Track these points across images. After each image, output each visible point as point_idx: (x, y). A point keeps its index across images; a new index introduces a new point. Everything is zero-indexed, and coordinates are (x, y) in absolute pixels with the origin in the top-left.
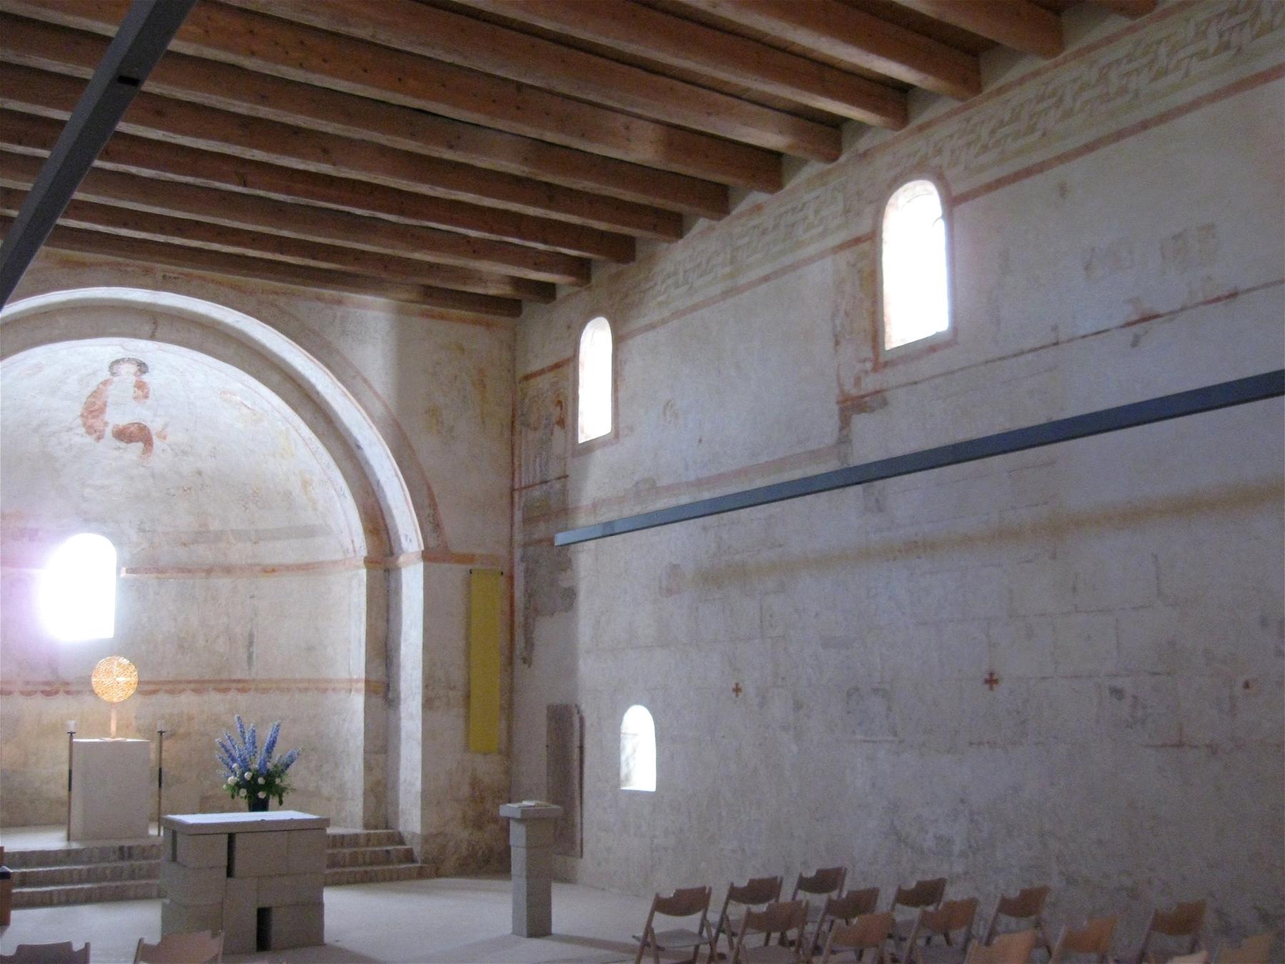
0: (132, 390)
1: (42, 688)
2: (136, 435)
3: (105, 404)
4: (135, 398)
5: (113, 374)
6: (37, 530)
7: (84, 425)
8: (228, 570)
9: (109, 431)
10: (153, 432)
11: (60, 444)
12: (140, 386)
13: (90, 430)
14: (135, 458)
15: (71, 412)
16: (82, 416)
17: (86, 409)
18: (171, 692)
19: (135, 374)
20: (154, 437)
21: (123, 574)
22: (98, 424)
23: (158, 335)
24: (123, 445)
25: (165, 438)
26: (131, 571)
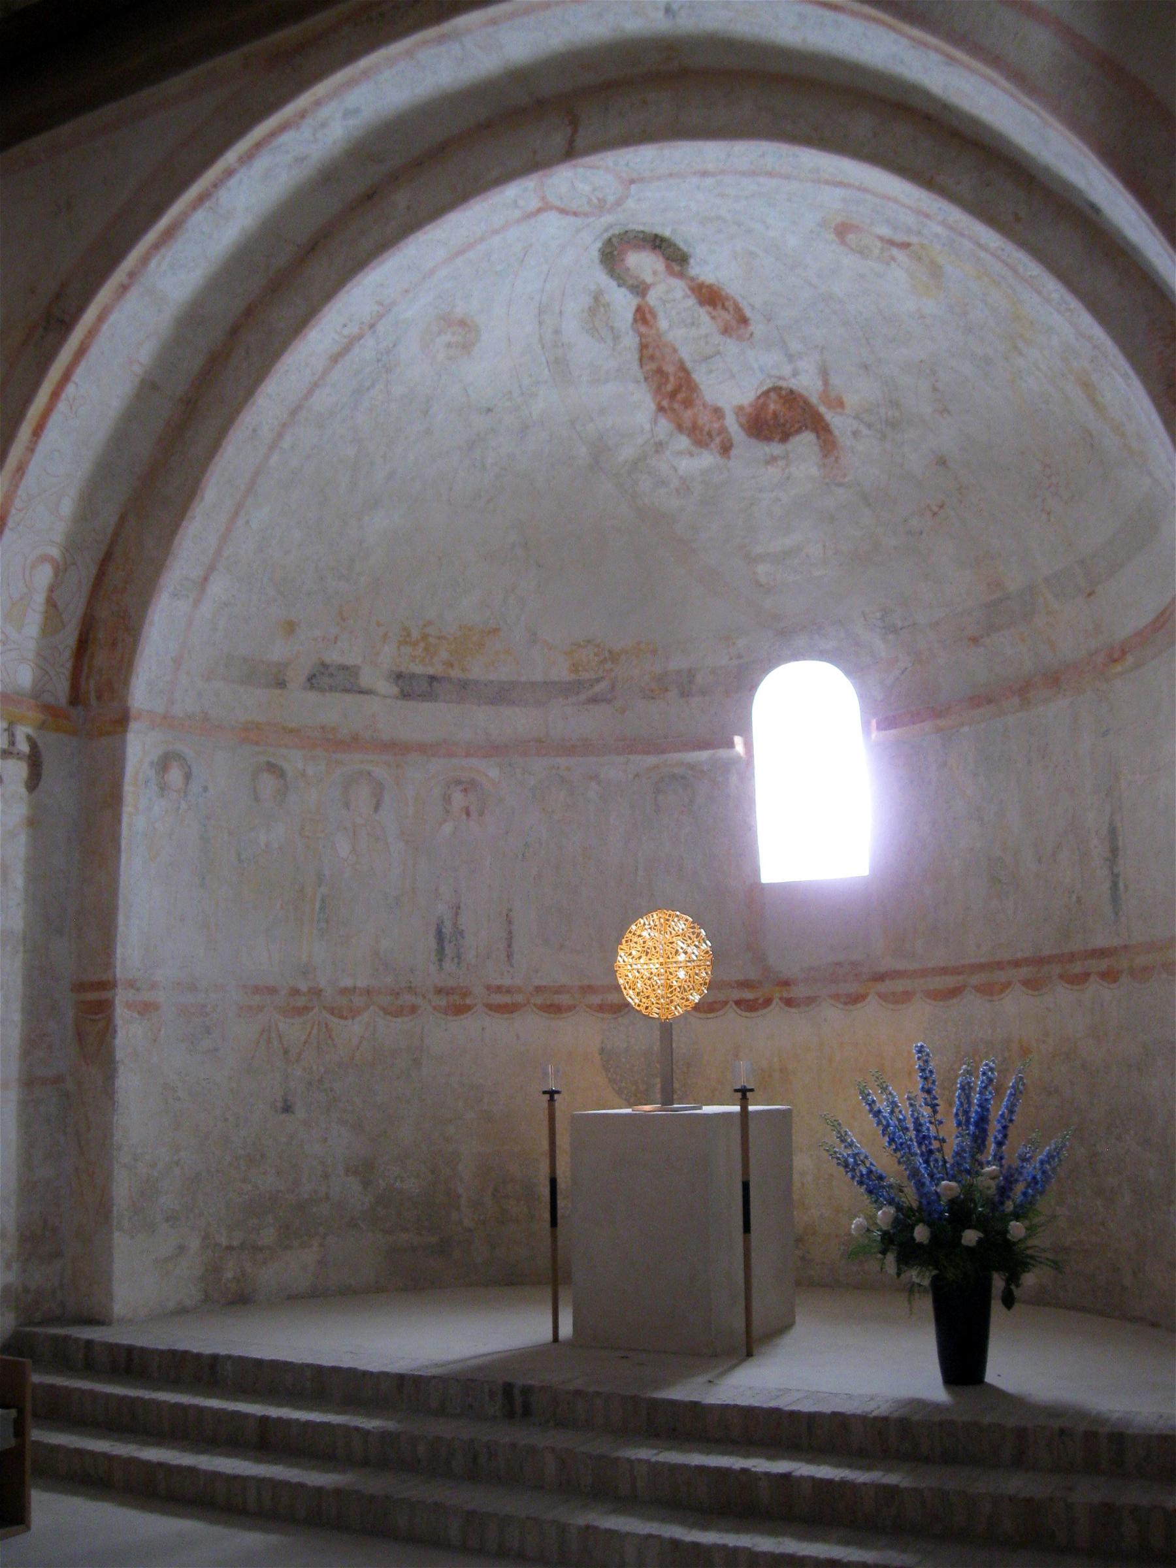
0: (703, 313)
1: (737, 994)
2: (782, 417)
3: (682, 367)
4: (726, 331)
5: (640, 289)
6: (691, 674)
7: (680, 428)
8: (1054, 679)
9: (732, 424)
10: (814, 400)
11: (663, 483)
12: (710, 297)
13: (700, 436)
14: (814, 471)
15: (636, 410)
16: (661, 409)
17: (658, 390)
18: (988, 990)
19: (671, 272)
20: (822, 409)
21: (874, 734)
22: (704, 419)
23: (579, 142)
24: (775, 448)
25: (841, 404)
26: (888, 723)
